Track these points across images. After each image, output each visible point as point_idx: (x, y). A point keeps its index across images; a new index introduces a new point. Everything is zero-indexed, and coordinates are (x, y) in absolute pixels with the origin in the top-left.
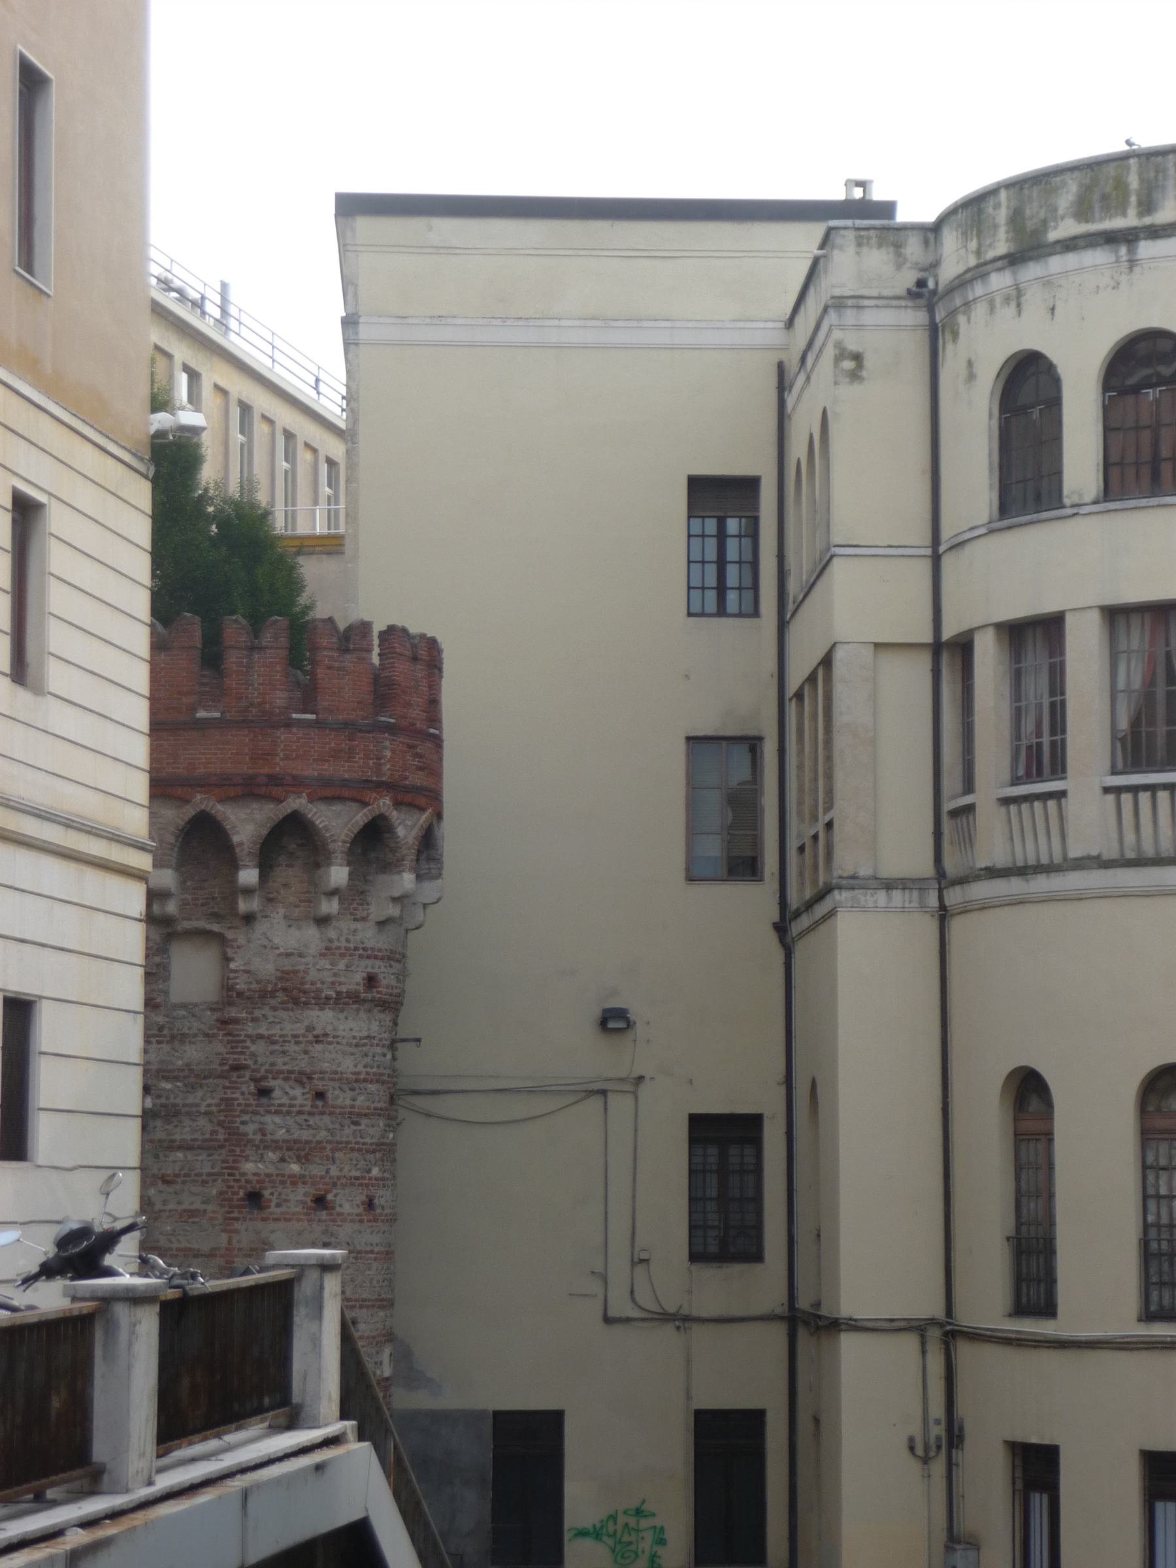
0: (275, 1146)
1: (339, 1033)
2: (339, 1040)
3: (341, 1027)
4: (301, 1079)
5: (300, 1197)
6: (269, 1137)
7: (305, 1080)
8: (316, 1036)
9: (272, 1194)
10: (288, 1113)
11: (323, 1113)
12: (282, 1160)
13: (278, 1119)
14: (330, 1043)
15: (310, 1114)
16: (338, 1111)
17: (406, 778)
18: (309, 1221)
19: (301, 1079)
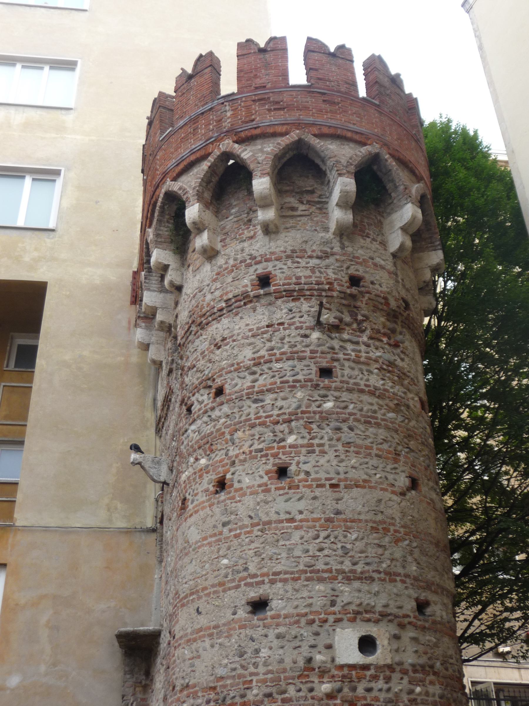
2: (235, 338)
7: (210, 383)
11: (222, 404)
16: (234, 397)
17: (253, 120)
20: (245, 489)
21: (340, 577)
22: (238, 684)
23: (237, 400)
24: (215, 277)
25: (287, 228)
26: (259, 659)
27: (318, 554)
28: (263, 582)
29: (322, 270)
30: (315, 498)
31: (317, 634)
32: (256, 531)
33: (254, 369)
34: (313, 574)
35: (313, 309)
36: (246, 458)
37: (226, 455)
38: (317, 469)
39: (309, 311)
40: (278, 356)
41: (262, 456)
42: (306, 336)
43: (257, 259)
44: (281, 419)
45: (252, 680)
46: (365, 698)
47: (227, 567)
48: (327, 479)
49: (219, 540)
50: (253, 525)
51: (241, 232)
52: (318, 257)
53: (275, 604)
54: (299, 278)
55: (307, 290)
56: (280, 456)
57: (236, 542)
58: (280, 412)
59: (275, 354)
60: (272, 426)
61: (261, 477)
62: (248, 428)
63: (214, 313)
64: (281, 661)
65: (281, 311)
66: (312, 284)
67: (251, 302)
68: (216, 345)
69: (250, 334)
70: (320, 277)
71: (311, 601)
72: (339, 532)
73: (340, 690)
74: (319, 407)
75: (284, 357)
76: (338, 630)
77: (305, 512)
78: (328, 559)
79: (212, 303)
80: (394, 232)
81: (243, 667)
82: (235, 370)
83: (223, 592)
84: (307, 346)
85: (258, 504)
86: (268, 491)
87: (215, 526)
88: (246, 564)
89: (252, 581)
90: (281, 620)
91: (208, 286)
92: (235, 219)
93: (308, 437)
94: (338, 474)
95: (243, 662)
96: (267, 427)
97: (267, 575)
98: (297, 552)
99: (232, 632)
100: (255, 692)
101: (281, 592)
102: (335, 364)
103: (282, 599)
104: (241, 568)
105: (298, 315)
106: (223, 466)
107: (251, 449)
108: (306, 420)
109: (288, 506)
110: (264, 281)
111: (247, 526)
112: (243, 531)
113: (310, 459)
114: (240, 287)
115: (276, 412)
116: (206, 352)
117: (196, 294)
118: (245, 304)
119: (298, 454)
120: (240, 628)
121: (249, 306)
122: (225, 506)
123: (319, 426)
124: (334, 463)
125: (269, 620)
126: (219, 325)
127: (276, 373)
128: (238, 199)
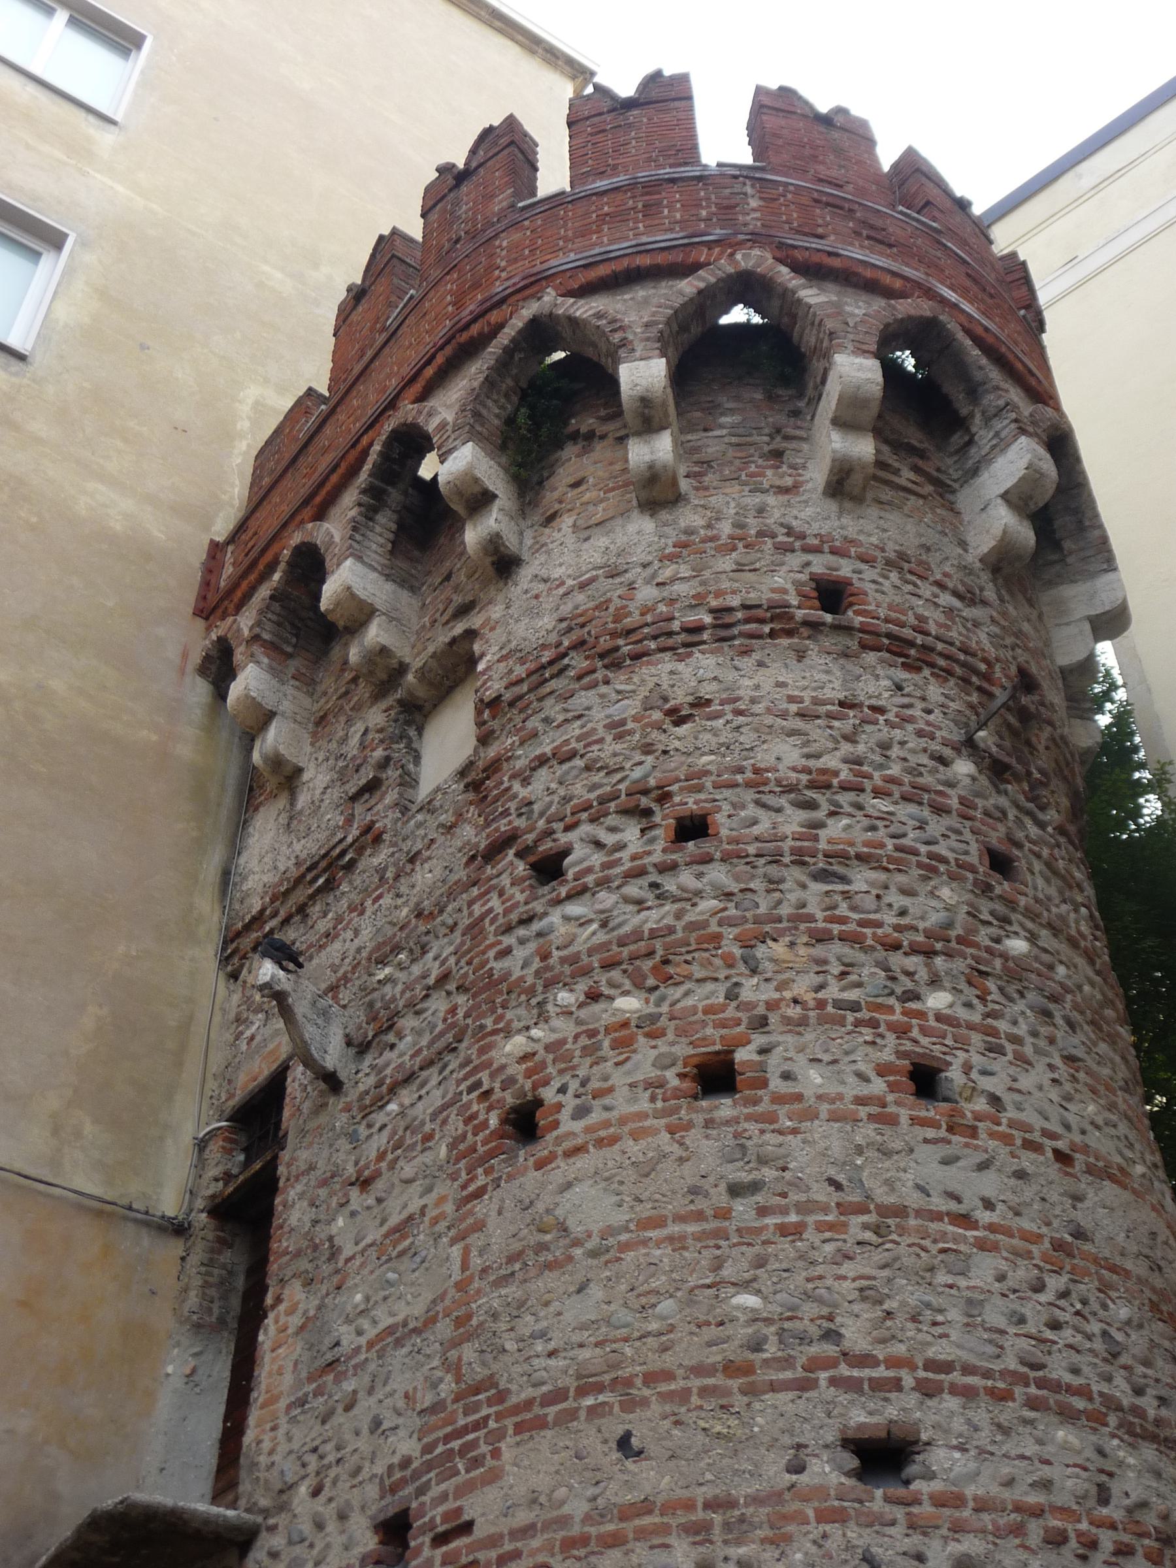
1: (741, 693)
5: (647, 1071)
8: (670, 712)
10: (603, 883)
11: (707, 860)
12: (594, 996)
13: (574, 909)
16: (752, 849)
23: (762, 861)
27: (1049, 1334)
28: (896, 1385)
30: (1021, 1175)
33: (810, 794)
41: (858, 1023)
42: (943, 761)
47: (755, 1318)
51: (753, 468)
52: (956, 594)
53: (943, 1464)
54: (921, 619)
55: (940, 654)
56: (915, 1033)
57: (785, 1247)
60: (881, 954)
61: (862, 1077)
62: (805, 939)
63: (670, 634)
65: (876, 681)
66: (952, 644)
67: (789, 633)
69: (794, 708)
71: (1046, 1471)
75: (896, 791)
77: (1000, 1207)
78: (1076, 1358)
80: (1067, 624)
82: (749, 785)
83: (744, 1393)
85: (859, 1150)
86: (891, 1121)
87: (694, 1191)
88: (830, 1318)
89: (856, 1373)
90: (966, 1513)
91: (645, 566)
92: (734, 440)
94: (1068, 1127)
96: (866, 950)
99: (791, 1528)
101: (958, 1425)
103: (962, 1449)
104: (814, 1331)
105: (920, 705)
106: (723, 1024)
107: (820, 995)
110: (831, 594)
111: (825, 1209)
112: (811, 1219)
117: (593, 580)
118: (773, 634)
119: (963, 1044)
122: (736, 1135)
125: (927, 1508)
126: (681, 667)
127: (880, 823)
128: (737, 398)
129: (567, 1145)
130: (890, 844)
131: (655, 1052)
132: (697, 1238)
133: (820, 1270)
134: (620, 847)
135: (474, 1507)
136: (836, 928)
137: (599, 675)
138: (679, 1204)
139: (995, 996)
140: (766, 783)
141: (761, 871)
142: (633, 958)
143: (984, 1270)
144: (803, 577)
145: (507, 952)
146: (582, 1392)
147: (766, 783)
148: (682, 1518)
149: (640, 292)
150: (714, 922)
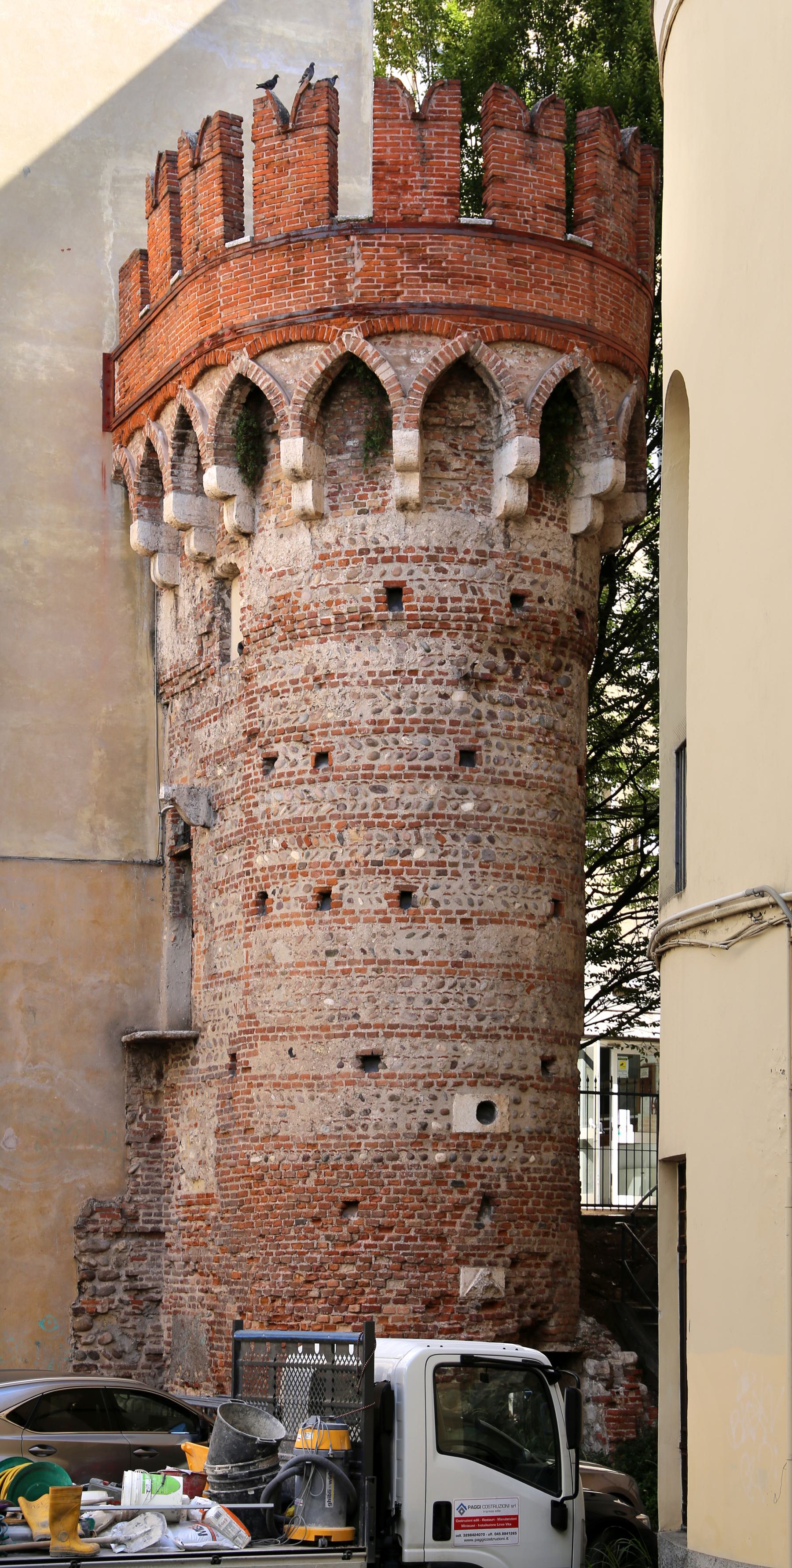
0: (275, 829)
2: (347, 679)
3: (350, 662)
4: (302, 735)
5: (301, 893)
6: (273, 818)
7: (307, 738)
9: (274, 893)
11: (326, 779)
14: (335, 685)
15: (312, 782)
16: (345, 775)
18: (308, 923)
19: (302, 735)
20: (357, 913)
21: (464, 1035)
22: (344, 1145)
23: (349, 782)
24: (317, 561)
25: (431, 503)
26: (367, 1122)
27: (442, 1006)
29: (476, 586)
30: (442, 936)
31: (434, 1098)
32: (370, 972)
33: (374, 737)
34: (436, 1031)
35: (457, 653)
36: (359, 871)
37: (332, 858)
38: (447, 897)
39: (453, 655)
40: (407, 724)
41: (380, 872)
43: (385, 554)
44: (407, 822)
45: (360, 1144)
46: (479, 1168)
48: (460, 912)
49: (322, 972)
50: (366, 962)
51: (361, 492)
52: (473, 562)
54: (443, 600)
56: (404, 875)
57: (343, 980)
58: (407, 812)
59: (403, 721)
64: (395, 1125)
68: (316, 679)
70: (472, 601)
72: (467, 980)
73: (454, 1159)
74: (455, 809)
76: (457, 1095)
79: (313, 608)
81: (350, 1127)
82: (347, 733)
84: (447, 712)
85: (374, 936)
86: (387, 921)
87: (315, 952)
93: (440, 852)
94: (472, 905)
95: (350, 1123)
97: (382, 1026)
98: (419, 1003)
100: (363, 1156)
101: (397, 1048)
102: (481, 742)
104: (351, 1015)
106: (327, 873)
108: (438, 827)
109: (410, 944)
110: (394, 594)
111: (359, 962)
112: (353, 967)
113: (441, 883)
114: (359, 597)
115: (401, 811)
116: (300, 684)
117: (282, 574)
118: (364, 627)
119: (426, 873)
120: (348, 1083)
121: (369, 632)
122: (330, 928)
123: (455, 837)
124: (469, 890)
125: (382, 1079)
126: (322, 647)
127: (404, 752)
129: (275, 921)
130: (407, 764)
131: (303, 884)
132: (316, 972)
133: (354, 989)
134: (295, 763)
135: (253, 1062)
136: (376, 820)
137: (288, 642)
138: (308, 959)
139: (449, 841)
140: (355, 731)
141: (348, 788)
142: (298, 830)
143: (419, 980)
144: (380, 586)
145: (256, 805)
146: (279, 1029)
147: (355, 731)
148: (306, 1081)
149: (294, 355)
150: (328, 816)
